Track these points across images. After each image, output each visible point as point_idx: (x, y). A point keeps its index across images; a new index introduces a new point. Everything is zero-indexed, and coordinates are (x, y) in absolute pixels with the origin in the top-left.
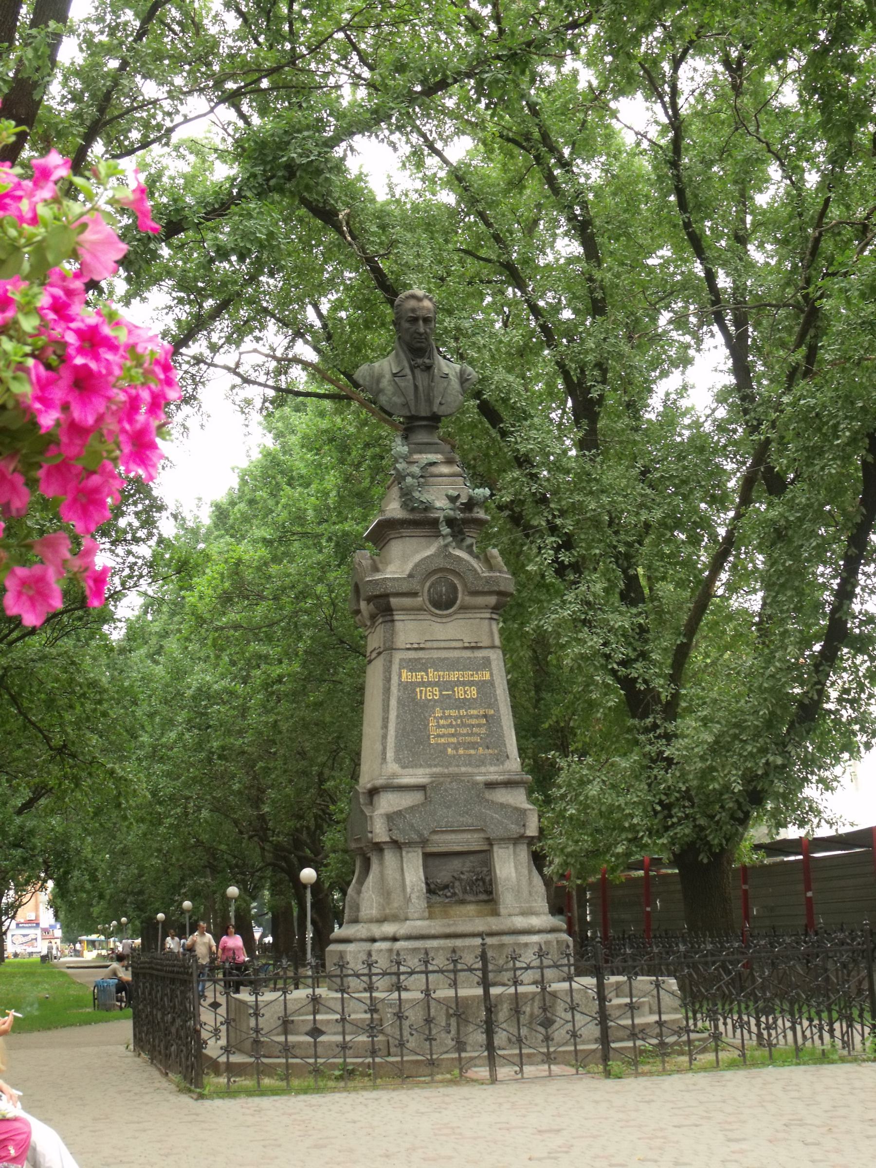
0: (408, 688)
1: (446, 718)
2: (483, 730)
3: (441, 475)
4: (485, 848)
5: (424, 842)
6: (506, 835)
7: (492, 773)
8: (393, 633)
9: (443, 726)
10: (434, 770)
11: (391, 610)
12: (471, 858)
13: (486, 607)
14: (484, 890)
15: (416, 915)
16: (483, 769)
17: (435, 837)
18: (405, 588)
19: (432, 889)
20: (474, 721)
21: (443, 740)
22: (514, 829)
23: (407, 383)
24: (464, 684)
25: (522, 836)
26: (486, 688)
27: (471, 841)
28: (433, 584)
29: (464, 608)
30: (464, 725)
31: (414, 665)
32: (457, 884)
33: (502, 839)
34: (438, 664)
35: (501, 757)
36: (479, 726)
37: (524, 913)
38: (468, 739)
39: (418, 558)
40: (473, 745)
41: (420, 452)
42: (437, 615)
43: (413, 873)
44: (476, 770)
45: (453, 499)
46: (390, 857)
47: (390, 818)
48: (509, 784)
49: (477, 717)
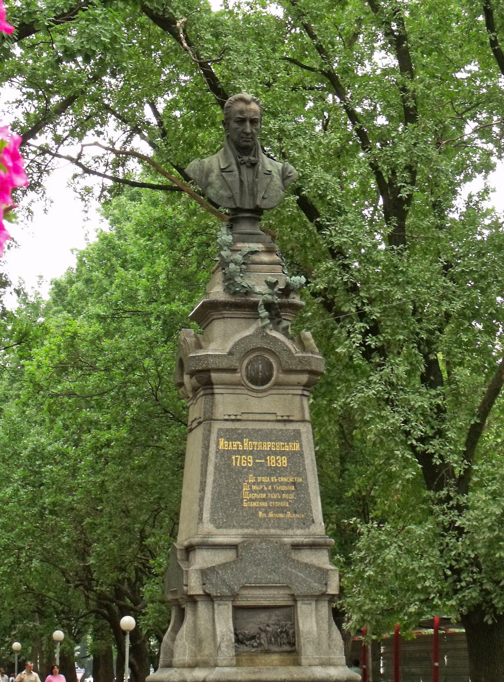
0: (225, 456)
1: (258, 484)
2: (292, 496)
3: (262, 263)
4: (290, 603)
5: (234, 596)
6: (309, 593)
7: (299, 535)
8: (212, 405)
9: (256, 491)
10: (246, 531)
11: (212, 384)
12: (277, 612)
13: (299, 384)
14: (288, 643)
15: (225, 663)
16: (290, 532)
17: (245, 592)
18: (224, 364)
19: (240, 639)
21: (255, 504)
22: (317, 587)
23: (233, 178)
24: (275, 453)
25: (324, 594)
26: (295, 458)
27: (279, 597)
28: (250, 363)
29: (279, 384)
30: (274, 491)
31: (231, 435)
32: (263, 635)
34: (253, 435)
35: (307, 522)
36: (288, 492)
37: (324, 664)
38: (278, 504)
39: (238, 337)
40: (282, 510)
41: (243, 242)
42: (253, 390)
43: (224, 625)
44: (284, 533)
45: (272, 285)
46: (202, 608)
47: (204, 573)
48: (313, 546)
49: (287, 484)
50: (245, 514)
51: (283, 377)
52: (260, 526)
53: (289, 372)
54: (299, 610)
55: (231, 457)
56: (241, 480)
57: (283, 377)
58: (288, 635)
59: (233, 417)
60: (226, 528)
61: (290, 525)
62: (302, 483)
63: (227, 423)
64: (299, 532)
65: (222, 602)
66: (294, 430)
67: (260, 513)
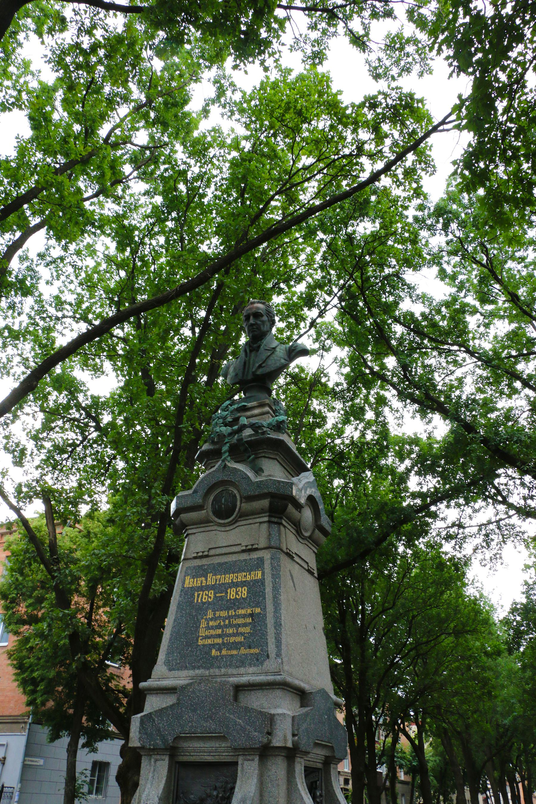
0: (189, 593)
9: (212, 628)
10: (197, 671)
13: (262, 511)
16: (242, 670)
20: (240, 621)
21: (209, 641)
22: (259, 738)
24: (236, 585)
29: (243, 515)
30: (231, 625)
33: (244, 749)
36: (245, 625)
38: (232, 639)
40: (236, 646)
44: (235, 671)
50: (198, 653)
51: (246, 506)
52: (212, 666)
53: (249, 499)
54: (239, 768)
55: (194, 594)
56: (199, 617)
57: (246, 506)
59: (200, 554)
60: (178, 670)
61: (242, 662)
62: (260, 613)
63: (196, 560)
64: (251, 670)
65: (158, 757)
66: (258, 559)
67: (214, 651)
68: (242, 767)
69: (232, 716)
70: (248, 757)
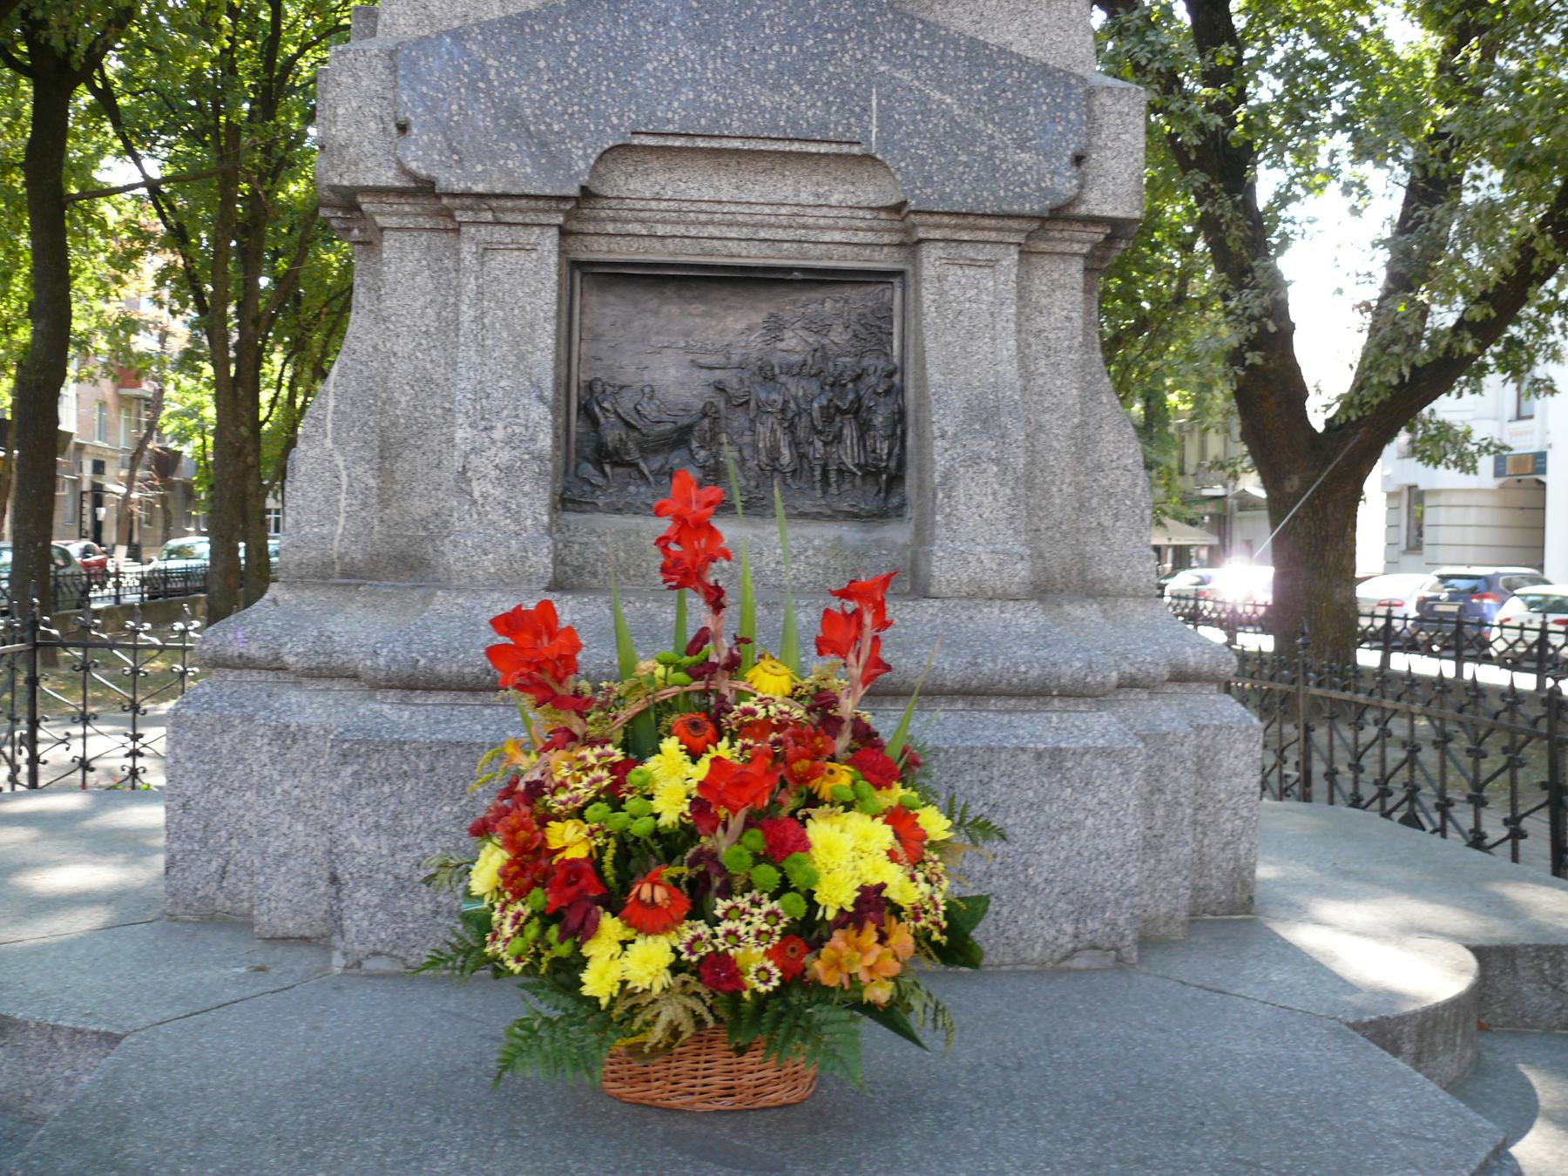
4: (882, 261)
54: (928, 296)
58: (864, 428)
65: (500, 234)
68: (942, 293)
69: (904, 76)
70: (970, 252)
